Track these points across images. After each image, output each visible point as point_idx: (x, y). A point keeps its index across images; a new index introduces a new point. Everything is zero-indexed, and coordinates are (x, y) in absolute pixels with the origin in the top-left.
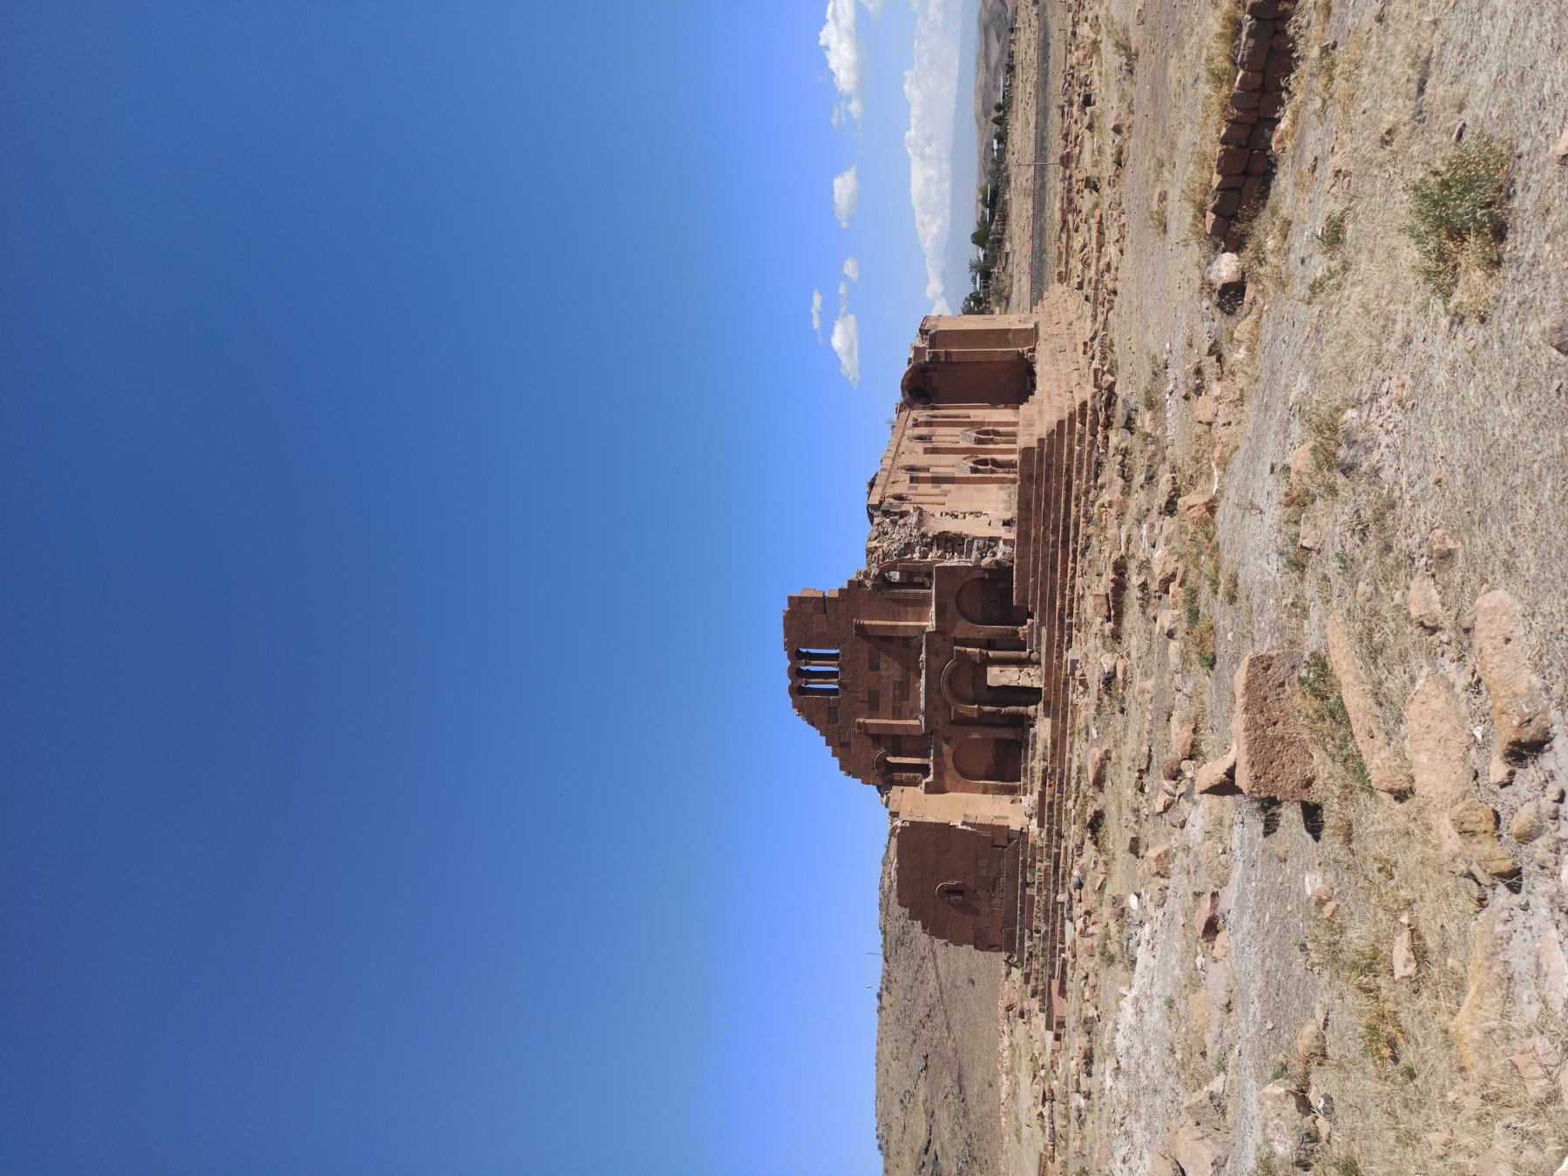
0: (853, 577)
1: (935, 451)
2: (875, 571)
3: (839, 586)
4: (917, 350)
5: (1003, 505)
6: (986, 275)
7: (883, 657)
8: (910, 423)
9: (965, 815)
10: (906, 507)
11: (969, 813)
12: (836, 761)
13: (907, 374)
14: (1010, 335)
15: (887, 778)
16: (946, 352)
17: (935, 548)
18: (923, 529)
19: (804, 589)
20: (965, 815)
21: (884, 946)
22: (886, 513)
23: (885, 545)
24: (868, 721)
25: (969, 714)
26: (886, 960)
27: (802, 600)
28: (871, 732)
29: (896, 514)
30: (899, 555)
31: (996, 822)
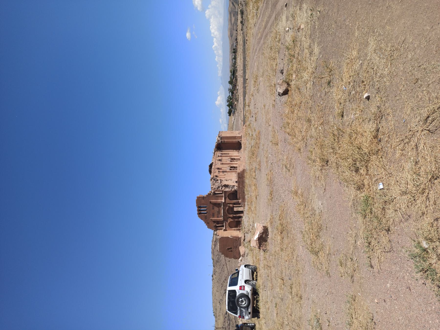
0: (209, 193)
1: (222, 164)
2: (213, 192)
3: (206, 194)
4: (218, 140)
5: (236, 178)
6: (233, 93)
7: (215, 207)
8: (217, 156)
9: (231, 235)
10: (218, 178)
11: (232, 235)
12: (207, 226)
13: (216, 145)
14: (236, 137)
15: (216, 228)
16: (224, 141)
17: (224, 187)
18: (221, 184)
19: (200, 195)
20: (231, 235)
21: (213, 263)
22: (214, 180)
23: (214, 186)
24: (212, 219)
25: (231, 217)
26: (214, 266)
27: (199, 197)
28: (213, 220)
29: (216, 180)
30: (217, 189)
31: (237, 236)
